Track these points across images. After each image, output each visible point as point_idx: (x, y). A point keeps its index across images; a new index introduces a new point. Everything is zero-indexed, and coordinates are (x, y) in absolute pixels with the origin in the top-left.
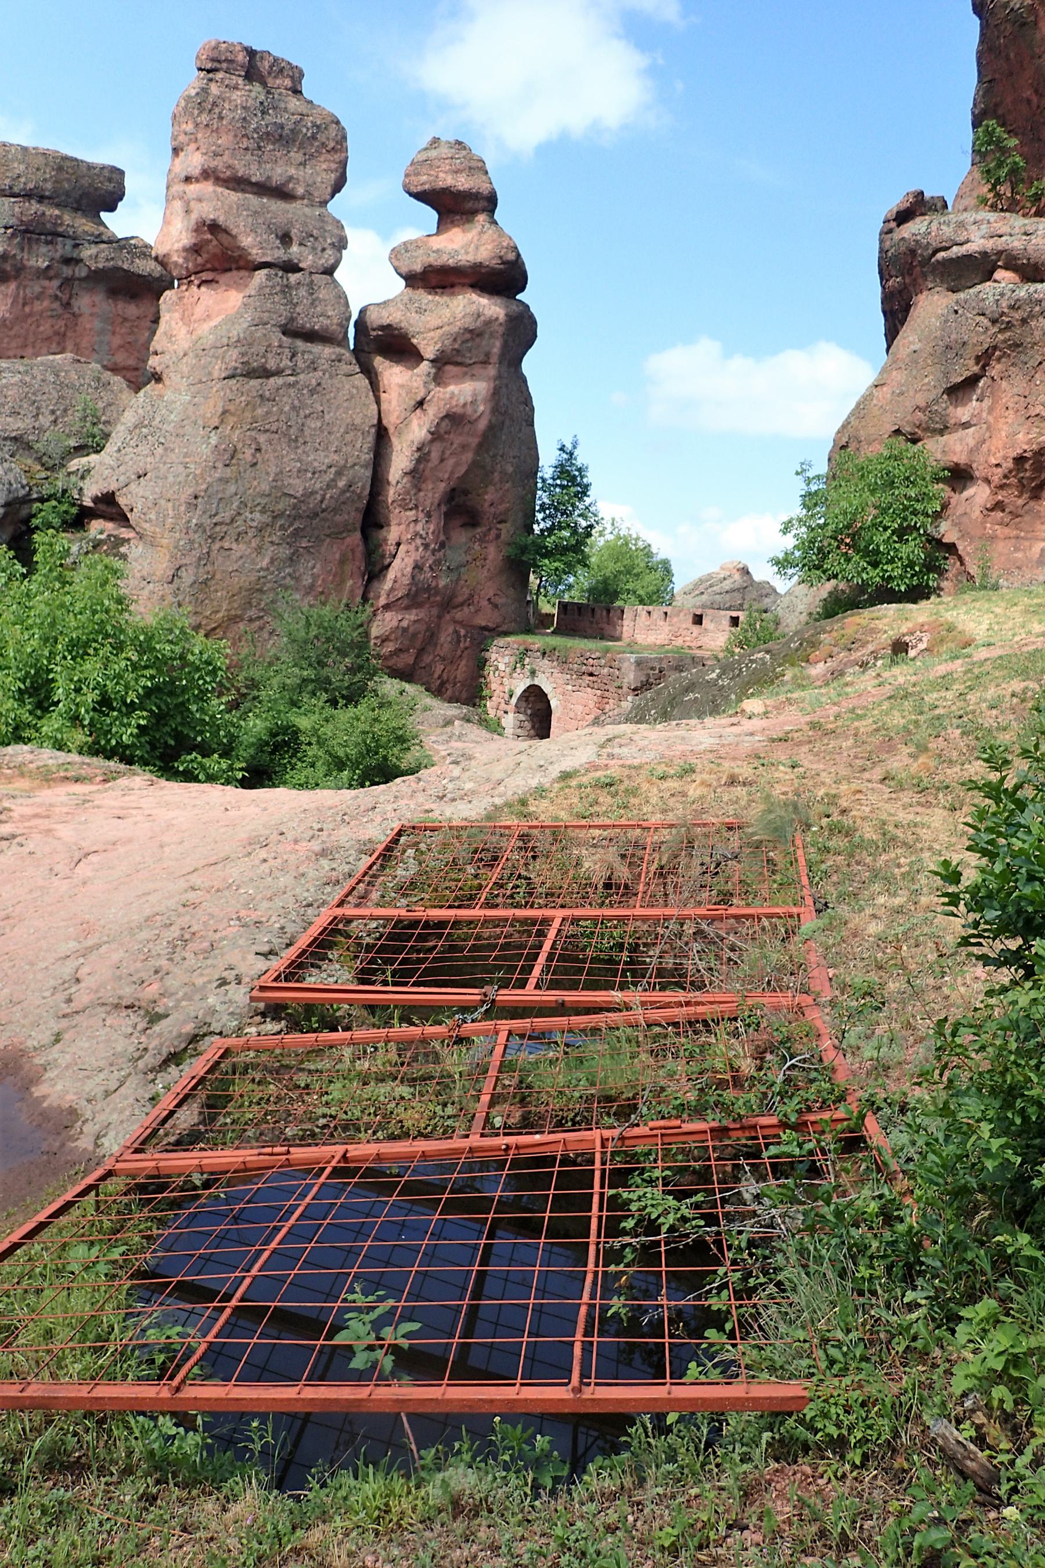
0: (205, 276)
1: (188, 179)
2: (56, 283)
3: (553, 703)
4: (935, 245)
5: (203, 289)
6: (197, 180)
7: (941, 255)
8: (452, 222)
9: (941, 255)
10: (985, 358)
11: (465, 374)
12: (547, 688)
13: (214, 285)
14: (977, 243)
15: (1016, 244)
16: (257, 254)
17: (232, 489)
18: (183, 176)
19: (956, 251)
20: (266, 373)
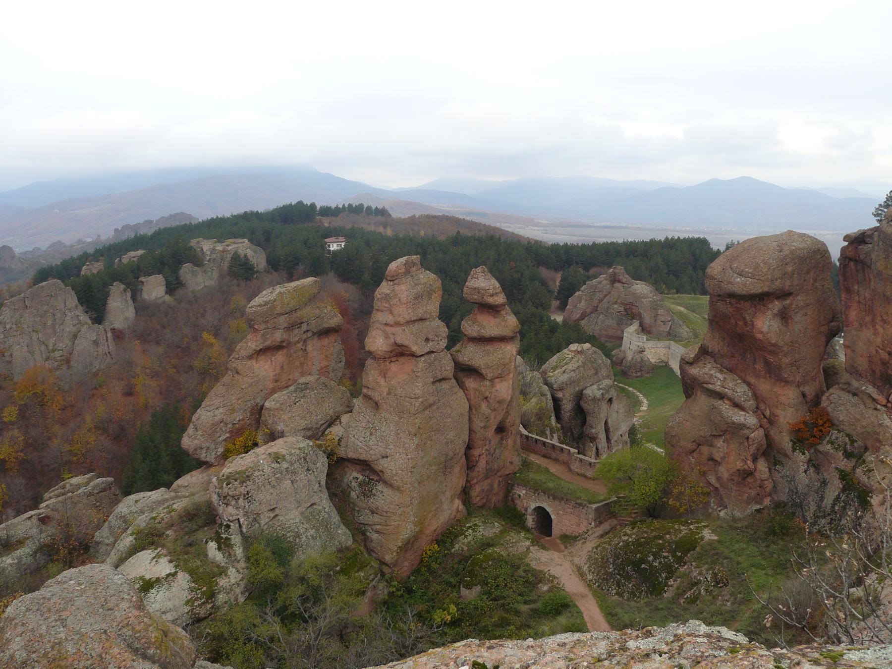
0: (393, 359)
1: (386, 324)
2: (301, 343)
3: (553, 517)
4: (702, 381)
5: (392, 364)
6: (392, 326)
7: (705, 385)
8: (488, 312)
9: (705, 385)
10: (725, 432)
11: (502, 380)
12: (549, 510)
13: (397, 362)
14: (718, 388)
15: (729, 392)
16: (419, 353)
17: (425, 460)
18: (385, 322)
19: (710, 386)
20: (430, 406)
